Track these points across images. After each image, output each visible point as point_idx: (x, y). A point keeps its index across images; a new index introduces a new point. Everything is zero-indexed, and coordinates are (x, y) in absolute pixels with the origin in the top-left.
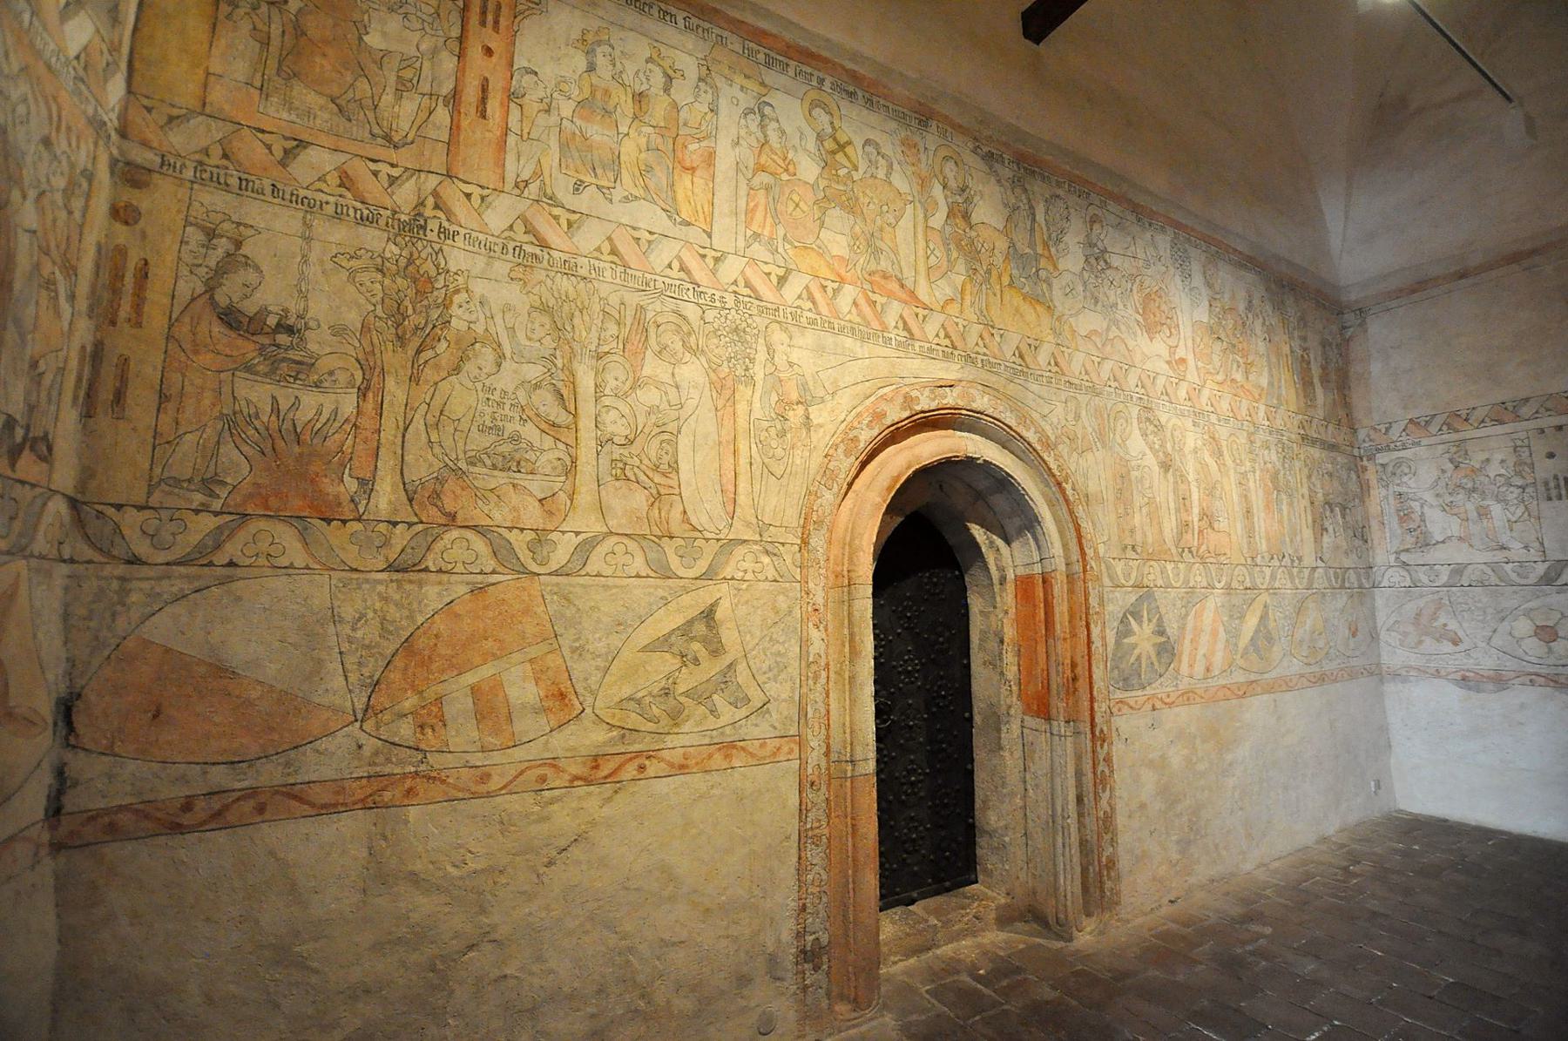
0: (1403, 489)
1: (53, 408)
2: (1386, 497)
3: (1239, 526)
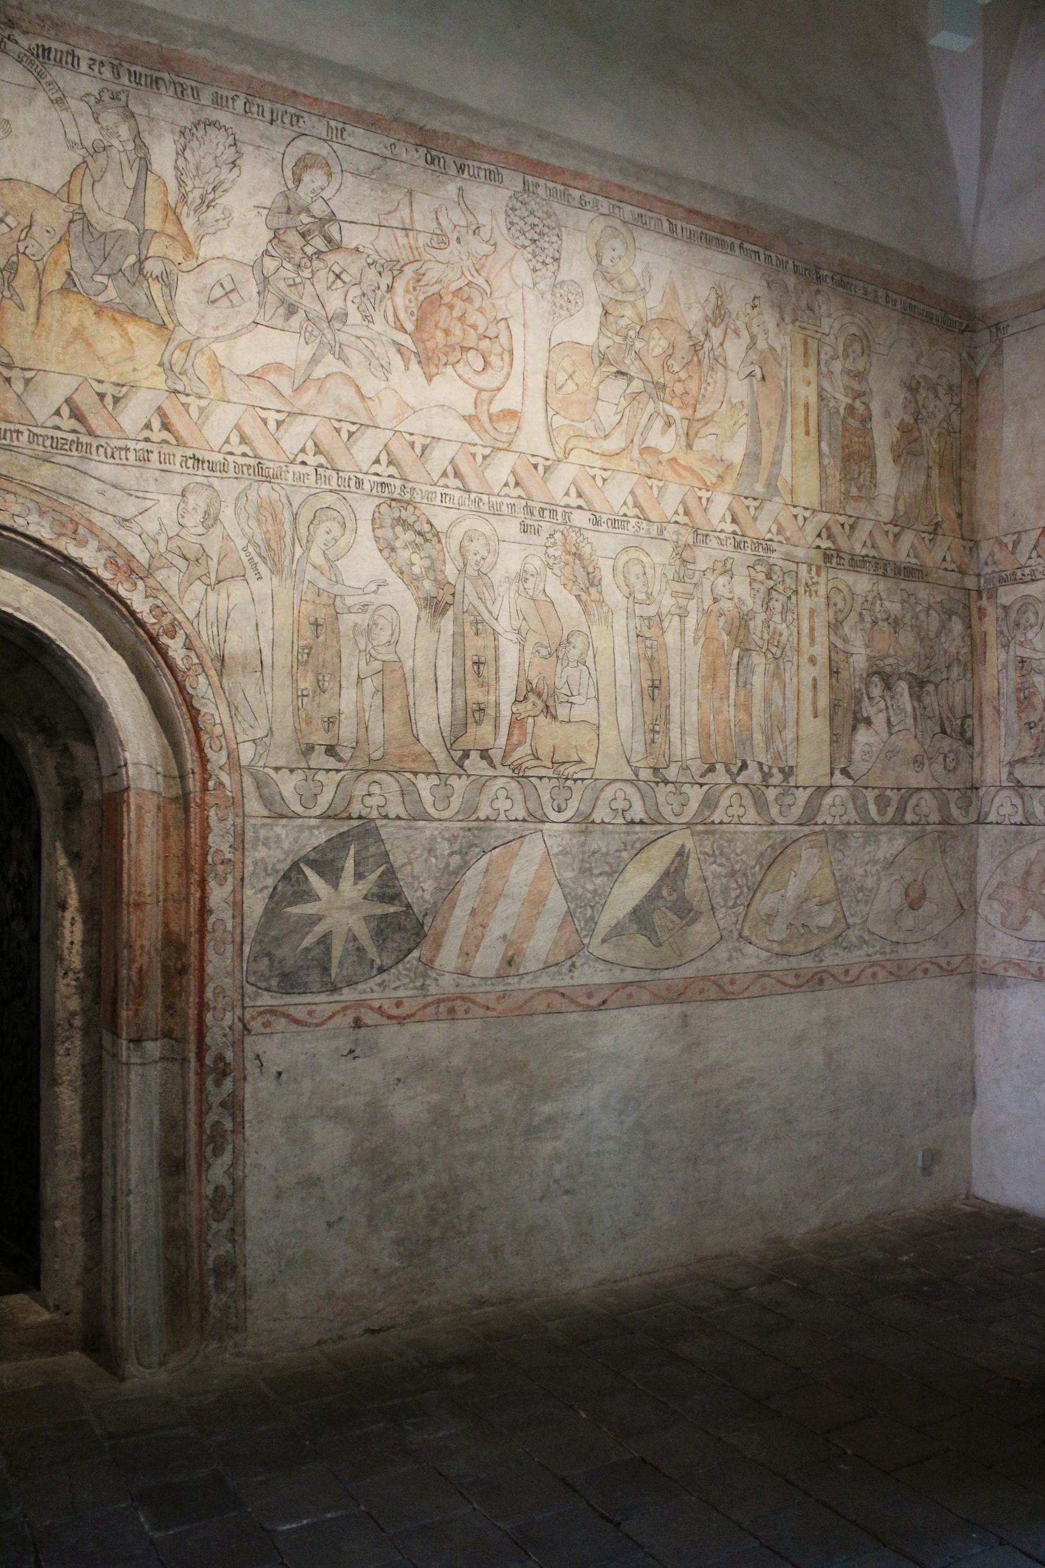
0: (1028, 653)
2: (1005, 666)
3: (625, 714)
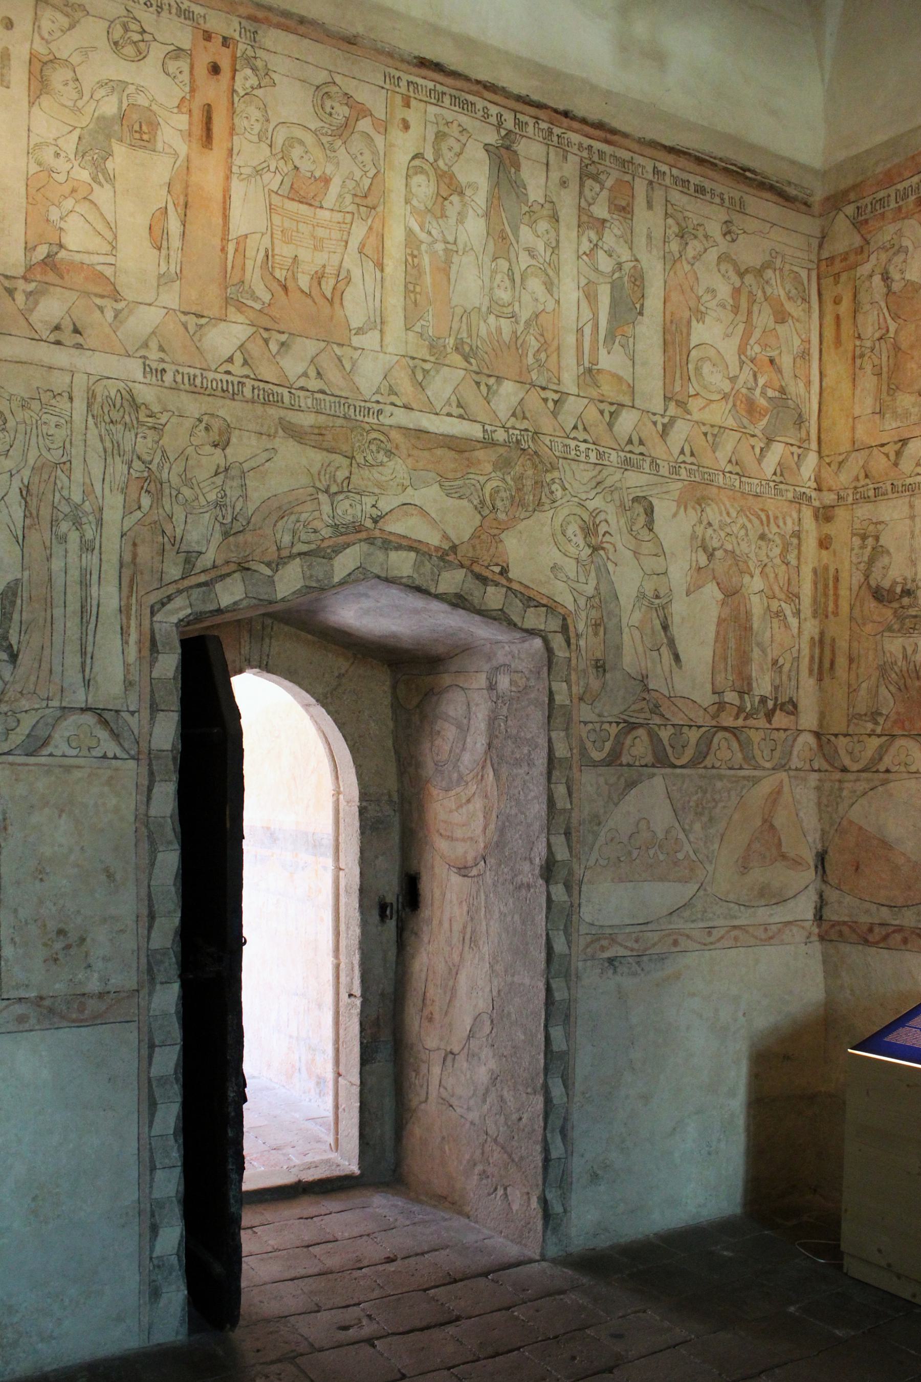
1: (793, 683)
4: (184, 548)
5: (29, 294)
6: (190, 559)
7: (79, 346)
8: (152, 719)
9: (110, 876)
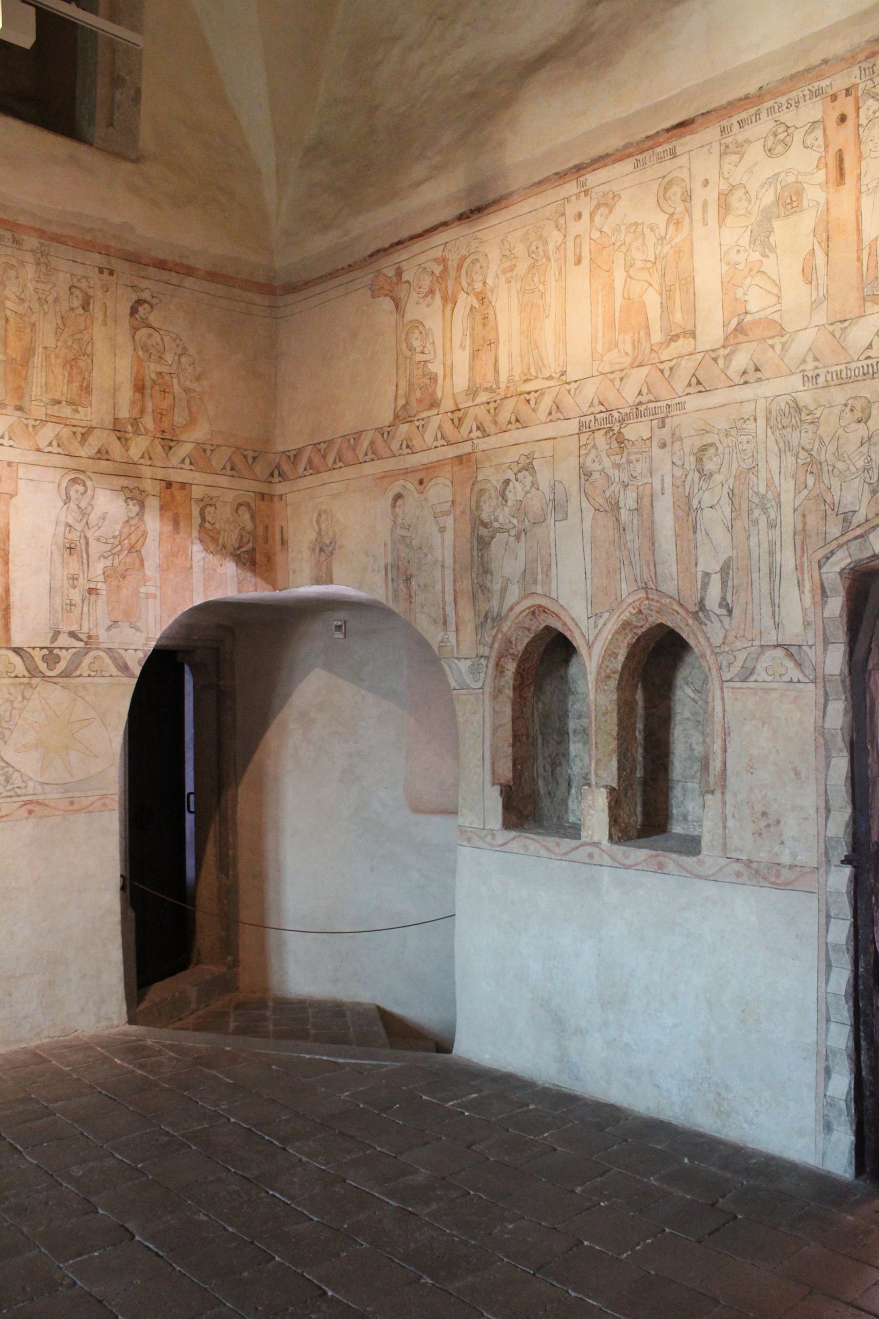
4: (841, 511)
5: (726, 357)
6: (846, 519)
7: (759, 380)
8: (825, 650)
9: (797, 774)
